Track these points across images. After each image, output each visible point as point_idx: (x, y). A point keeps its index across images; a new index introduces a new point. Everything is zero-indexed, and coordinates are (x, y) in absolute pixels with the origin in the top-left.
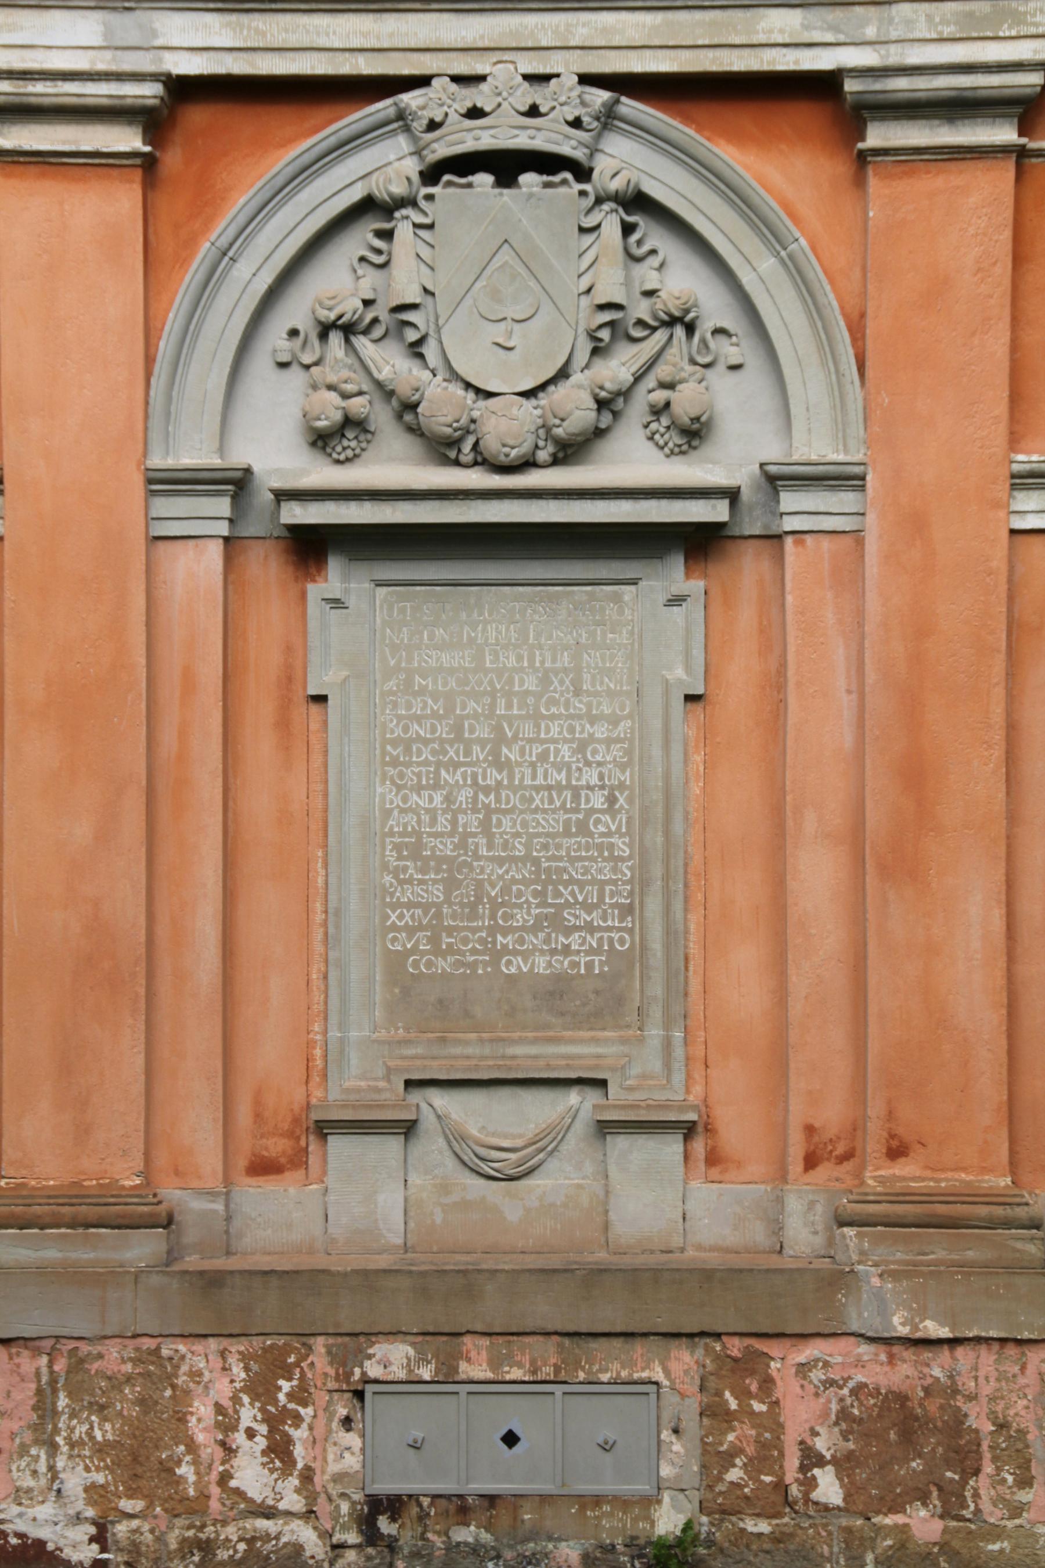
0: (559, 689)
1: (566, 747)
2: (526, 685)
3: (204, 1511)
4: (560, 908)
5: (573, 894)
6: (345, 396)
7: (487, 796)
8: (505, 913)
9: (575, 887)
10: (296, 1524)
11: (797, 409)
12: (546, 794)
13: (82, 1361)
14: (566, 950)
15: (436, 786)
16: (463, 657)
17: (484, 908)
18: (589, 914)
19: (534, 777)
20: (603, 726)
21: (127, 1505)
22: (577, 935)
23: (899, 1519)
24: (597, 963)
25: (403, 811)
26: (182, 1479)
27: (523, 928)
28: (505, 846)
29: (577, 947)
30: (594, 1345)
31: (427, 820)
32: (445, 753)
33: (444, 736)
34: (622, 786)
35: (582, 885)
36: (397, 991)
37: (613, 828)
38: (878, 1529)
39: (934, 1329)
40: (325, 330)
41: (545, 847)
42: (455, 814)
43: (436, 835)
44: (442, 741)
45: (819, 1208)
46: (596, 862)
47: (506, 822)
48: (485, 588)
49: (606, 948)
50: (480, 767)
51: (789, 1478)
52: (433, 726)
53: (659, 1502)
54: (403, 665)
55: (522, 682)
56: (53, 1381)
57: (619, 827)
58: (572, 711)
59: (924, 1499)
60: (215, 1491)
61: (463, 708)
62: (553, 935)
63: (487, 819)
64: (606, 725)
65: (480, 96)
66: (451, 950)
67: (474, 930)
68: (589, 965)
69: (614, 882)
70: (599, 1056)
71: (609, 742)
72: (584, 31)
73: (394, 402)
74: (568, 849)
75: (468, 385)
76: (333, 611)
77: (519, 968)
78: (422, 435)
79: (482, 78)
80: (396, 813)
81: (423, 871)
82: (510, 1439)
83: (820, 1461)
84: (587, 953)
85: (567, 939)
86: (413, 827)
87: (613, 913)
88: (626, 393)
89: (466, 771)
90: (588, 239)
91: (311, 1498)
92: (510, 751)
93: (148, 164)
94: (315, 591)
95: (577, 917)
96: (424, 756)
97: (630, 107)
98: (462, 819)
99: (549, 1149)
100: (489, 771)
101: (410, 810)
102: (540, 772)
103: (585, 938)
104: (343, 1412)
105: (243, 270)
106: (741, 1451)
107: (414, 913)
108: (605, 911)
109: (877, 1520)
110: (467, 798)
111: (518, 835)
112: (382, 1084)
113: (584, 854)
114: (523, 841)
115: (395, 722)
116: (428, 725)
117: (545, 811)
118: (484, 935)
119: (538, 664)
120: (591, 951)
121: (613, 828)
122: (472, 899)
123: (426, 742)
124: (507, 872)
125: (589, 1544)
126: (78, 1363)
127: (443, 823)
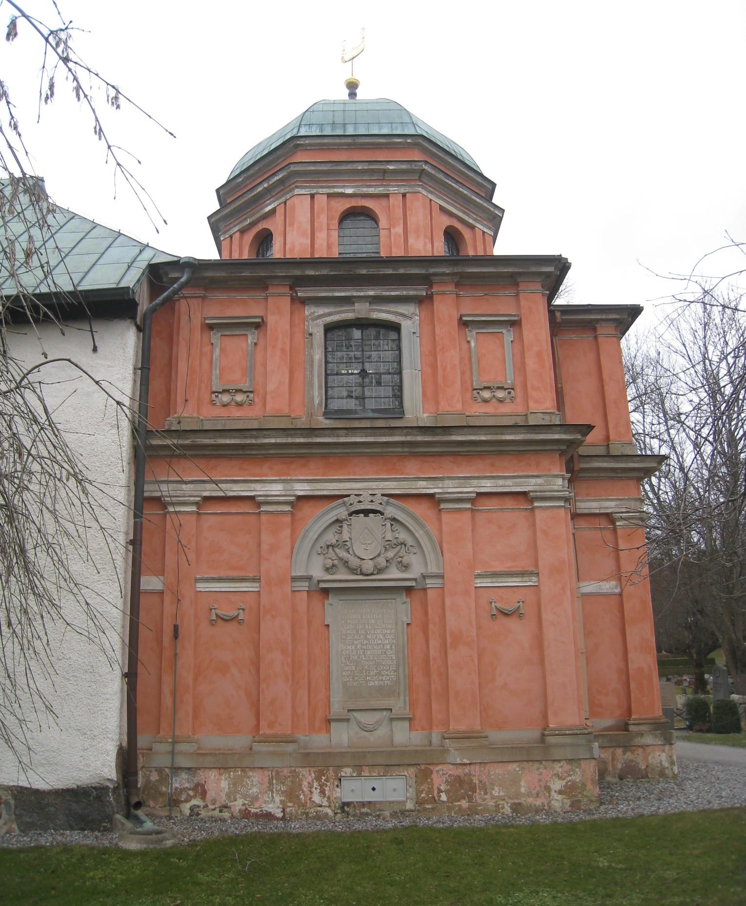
3: (306, 806)
4: (380, 671)
6: (333, 560)
10: (327, 808)
11: (428, 562)
13: (278, 773)
14: (382, 680)
15: (353, 644)
21: (289, 804)
23: (459, 803)
25: (346, 650)
26: (301, 799)
30: (393, 767)
35: (385, 665)
38: (455, 805)
39: (466, 761)
40: (328, 547)
45: (439, 736)
47: (369, 652)
51: (435, 796)
53: (407, 802)
56: (272, 777)
59: (464, 799)
60: (308, 801)
65: (361, 498)
66: (356, 681)
68: (387, 683)
71: (390, 634)
72: (382, 485)
73: (343, 561)
75: (359, 557)
78: (349, 568)
79: (361, 495)
82: (374, 789)
83: (442, 792)
88: (392, 559)
90: (384, 527)
91: (330, 803)
93: (292, 514)
94: (326, 602)
97: (392, 500)
104: (336, 784)
105: (311, 534)
106: (424, 790)
109: (454, 803)
120: (389, 680)
123: (351, 635)
125: (391, 811)
126: (278, 773)
127: (354, 653)
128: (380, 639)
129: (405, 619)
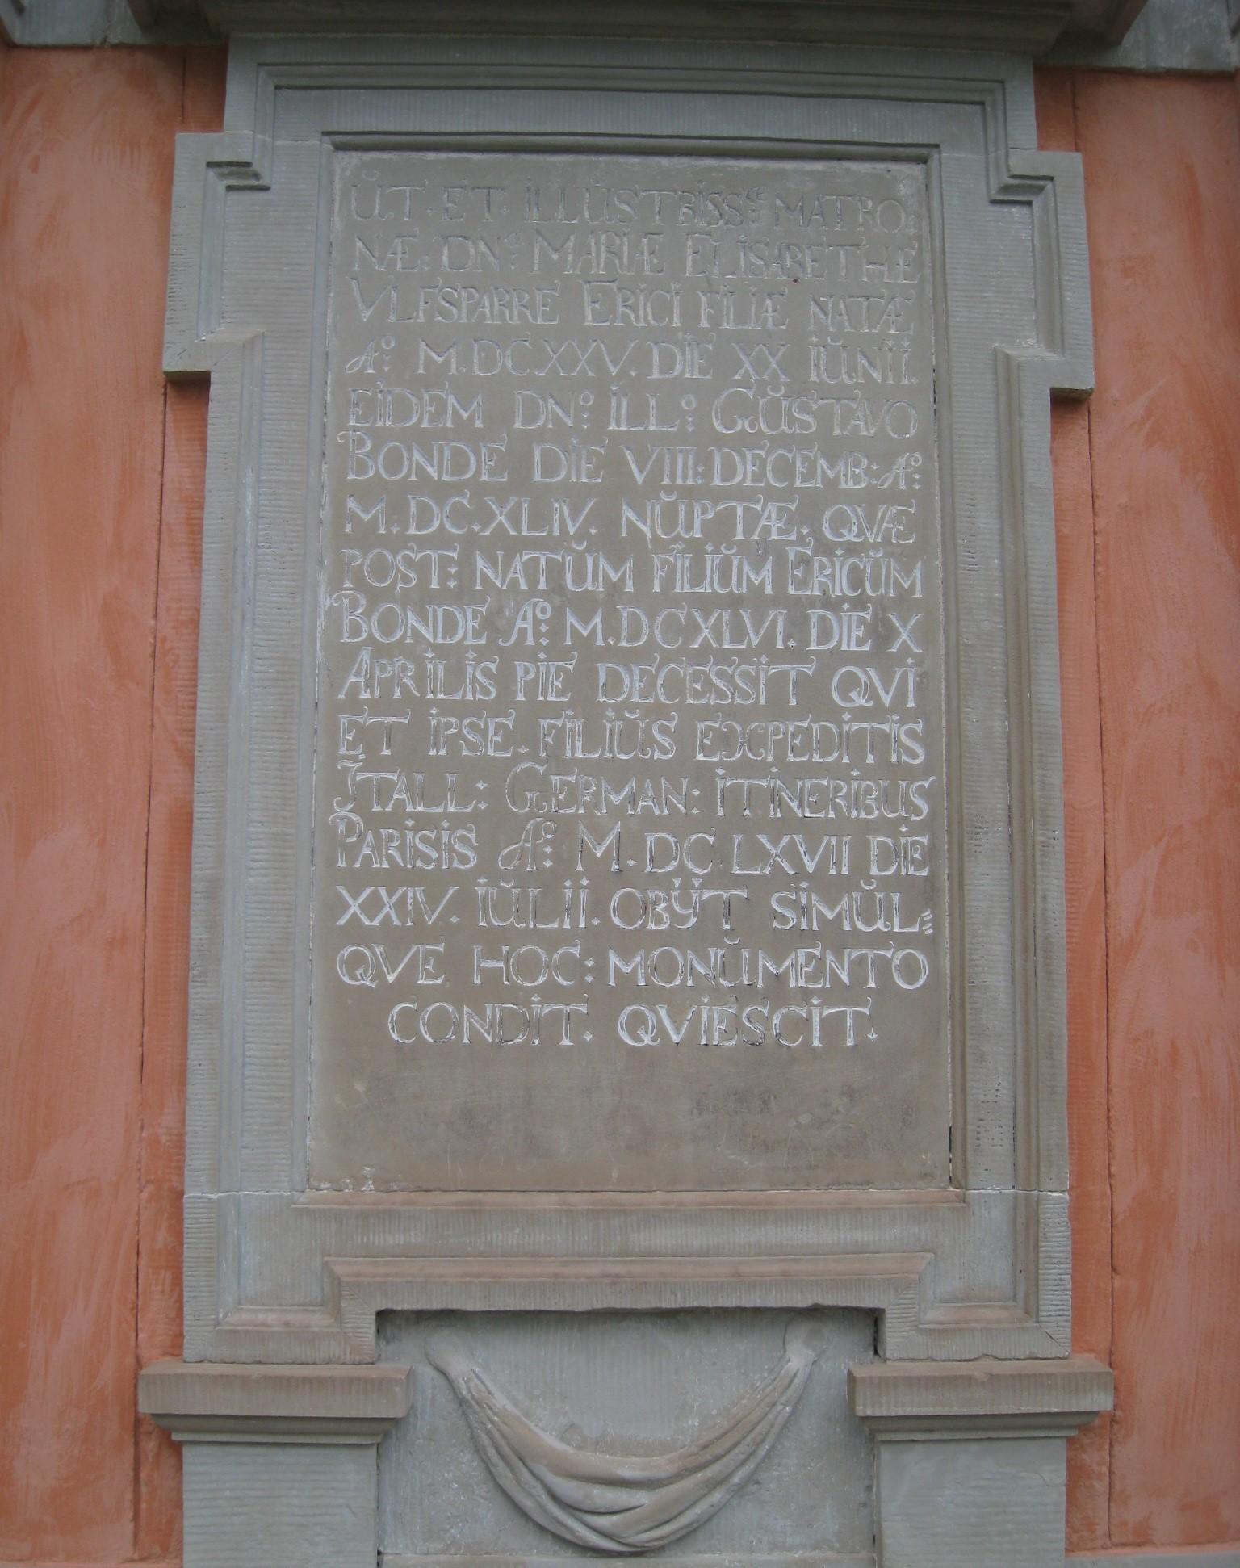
0: (754, 378)
1: (772, 508)
2: (678, 368)
5: (791, 853)
7: (585, 620)
8: (629, 897)
9: (798, 838)
12: (726, 616)
14: (777, 990)
15: (463, 594)
16: (532, 305)
17: (577, 887)
18: (832, 903)
19: (698, 577)
20: (857, 464)
22: (802, 954)
24: (850, 1022)
27: (672, 937)
28: (628, 736)
29: (802, 983)
31: (441, 674)
32: (487, 517)
33: (484, 478)
34: (904, 600)
35: (812, 831)
36: (360, 1087)
37: (887, 699)
41: (725, 741)
42: (507, 659)
43: (461, 710)
44: (479, 490)
46: (848, 779)
47: (632, 683)
48: (583, 158)
49: (872, 985)
50: (570, 551)
52: (458, 454)
54: (392, 319)
55: (667, 364)
57: (901, 695)
58: (785, 428)
61: (531, 416)
62: (745, 954)
63: (586, 672)
64: (865, 462)
66: (493, 987)
67: (553, 941)
68: (831, 1027)
69: (891, 827)
70: (859, 1250)
71: (872, 500)
74: (780, 747)
76: (234, 196)
77: (661, 1032)
80: (365, 655)
81: (425, 795)
84: (827, 997)
85: (778, 963)
86: (405, 689)
87: (889, 900)
89: (536, 560)
92: (642, 516)
95: (804, 910)
96: (436, 524)
98: (524, 672)
99: (736, 1479)
100: (590, 561)
101: (400, 648)
102: (712, 562)
103: (822, 960)
107: (404, 898)
108: (870, 896)
110: (537, 622)
111: (658, 711)
112: (319, 1320)
113: (817, 759)
114: (672, 725)
115: (369, 446)
116: (447, 454)
117: (724, 656)
118: (576, 952)
119: (704, 323)
120: (837, 993)
121: (887, 699)
122: (548, 864)
123: (441, 492)
124: (633, 800)
127: (477, 684)
128: (759, 552)
129: (1029, 347)
